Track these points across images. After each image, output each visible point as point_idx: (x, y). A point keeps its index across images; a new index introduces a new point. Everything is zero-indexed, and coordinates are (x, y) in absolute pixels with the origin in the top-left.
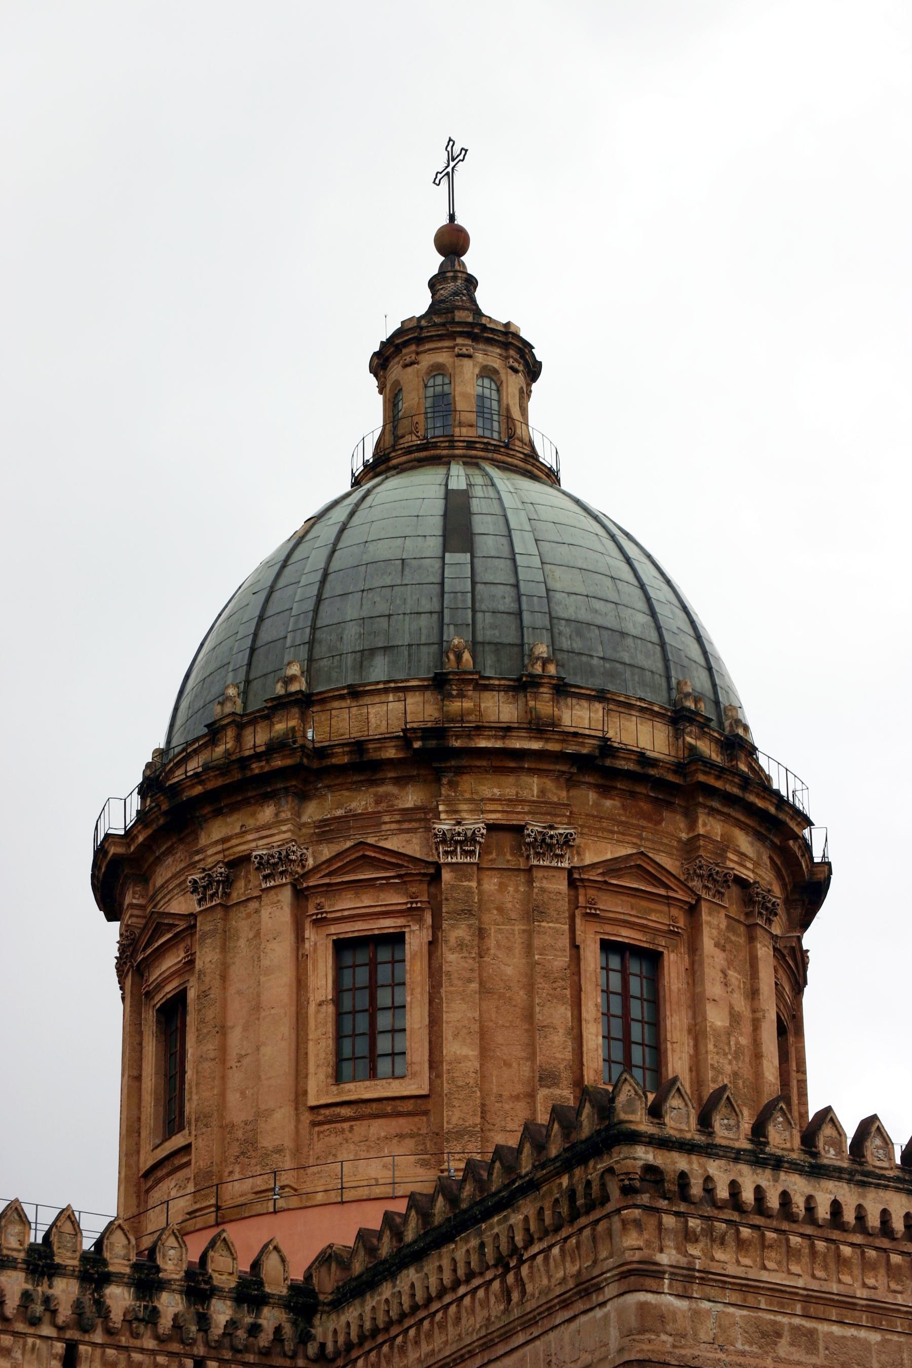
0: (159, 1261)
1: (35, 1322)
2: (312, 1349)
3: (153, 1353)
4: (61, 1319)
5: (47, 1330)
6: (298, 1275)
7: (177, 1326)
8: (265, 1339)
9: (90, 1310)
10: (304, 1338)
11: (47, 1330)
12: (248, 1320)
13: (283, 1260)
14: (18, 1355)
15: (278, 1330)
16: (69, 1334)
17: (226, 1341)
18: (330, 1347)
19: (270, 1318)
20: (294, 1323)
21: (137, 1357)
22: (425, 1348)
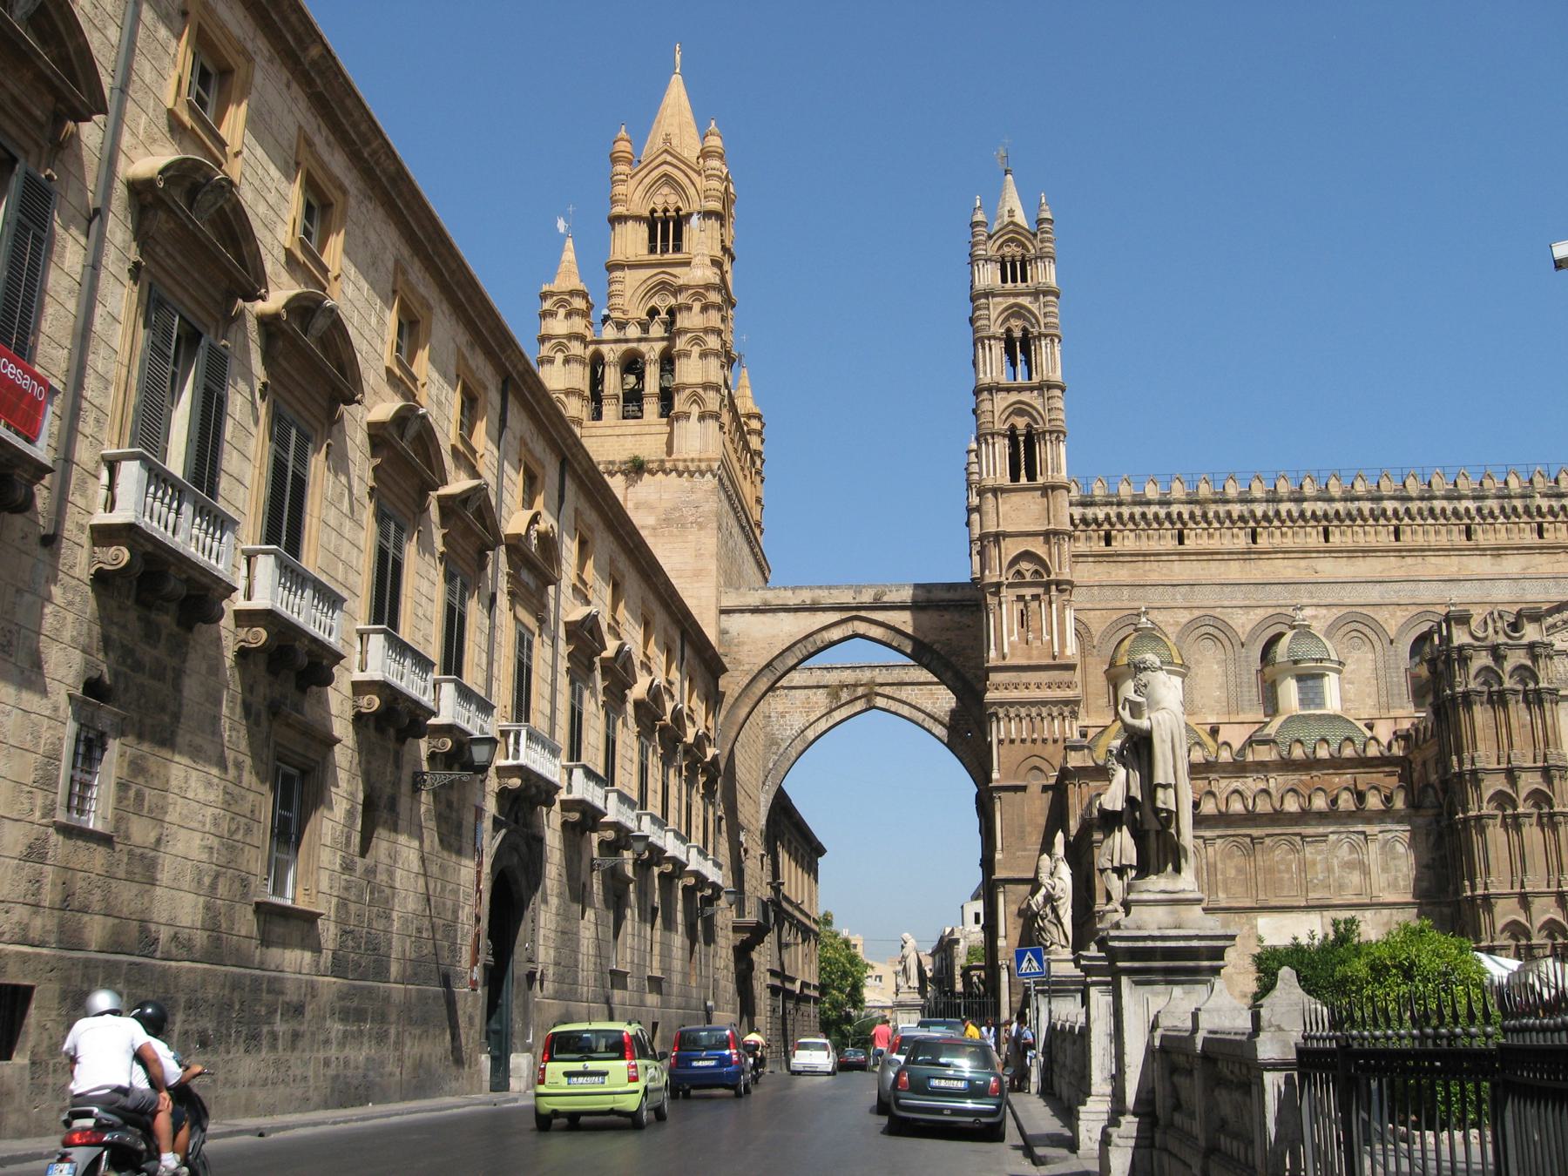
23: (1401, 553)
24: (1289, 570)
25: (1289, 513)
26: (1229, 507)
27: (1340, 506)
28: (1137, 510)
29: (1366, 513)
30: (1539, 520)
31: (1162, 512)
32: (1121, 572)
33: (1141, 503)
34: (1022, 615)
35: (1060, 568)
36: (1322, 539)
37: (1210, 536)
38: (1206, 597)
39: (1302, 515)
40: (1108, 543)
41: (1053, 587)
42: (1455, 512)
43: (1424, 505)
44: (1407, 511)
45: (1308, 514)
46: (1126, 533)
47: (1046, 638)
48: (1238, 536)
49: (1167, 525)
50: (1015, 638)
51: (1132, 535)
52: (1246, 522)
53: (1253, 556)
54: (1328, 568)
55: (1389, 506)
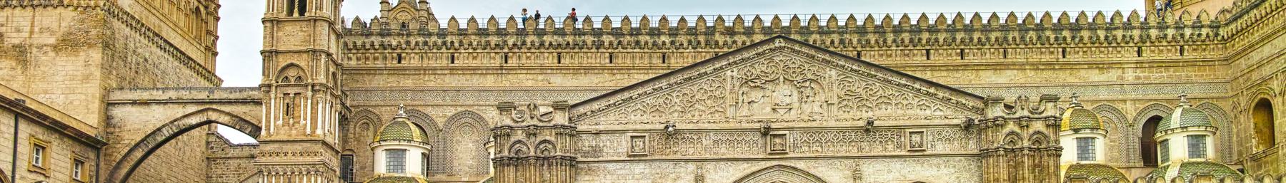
0: (1166, 20)
1: (1127, 43)
2: (1219, 38)
3: (1166, 46)
4: (1135, 41)
5: (1131, 44)
6: (1213, 18)
7: (1173, 37)
8: (1203, 37)
9: (1145, 38)
10: (1217, 35)
11: (1131, 44)
12: (1197, 33)
13: (1208, 14)
14: (1123, 52)
15: (1207, 34)
16: (1138, 45)
17: (1190, 40)
18: (1226, 37)
19: (1204, 31)
20: (1212, 31)
21: (1161, 48)
22: (1261, 32)
23: (612, 71)
24: (530, 81)
25: (532, 43)
26: (490, 38)
27: (570, 39)
28: (421, 39)
29: (589, 43)
30: (717, 50)
31: (440, 42)
32: (407, 81)
33: (424, 35)
34: (288, 107)
35: (316, 76)
36: (556, 61)
37: (474, 58)
38: (469, 100)
39: (542, 44)
40: (399, 62)
41: (310, 87)
42: (655, 44)
43: (633, 39)
44: (620, 42)
45: (547, 44)
46: (413, 55)
47: (302, 122)
48: (494, 58)
49: (444, 50)
50: (280, 122)
51: (417, 57)
52: (503, 48)
53: (504, 71)
54: (558, 80)
55: (606, 39)
